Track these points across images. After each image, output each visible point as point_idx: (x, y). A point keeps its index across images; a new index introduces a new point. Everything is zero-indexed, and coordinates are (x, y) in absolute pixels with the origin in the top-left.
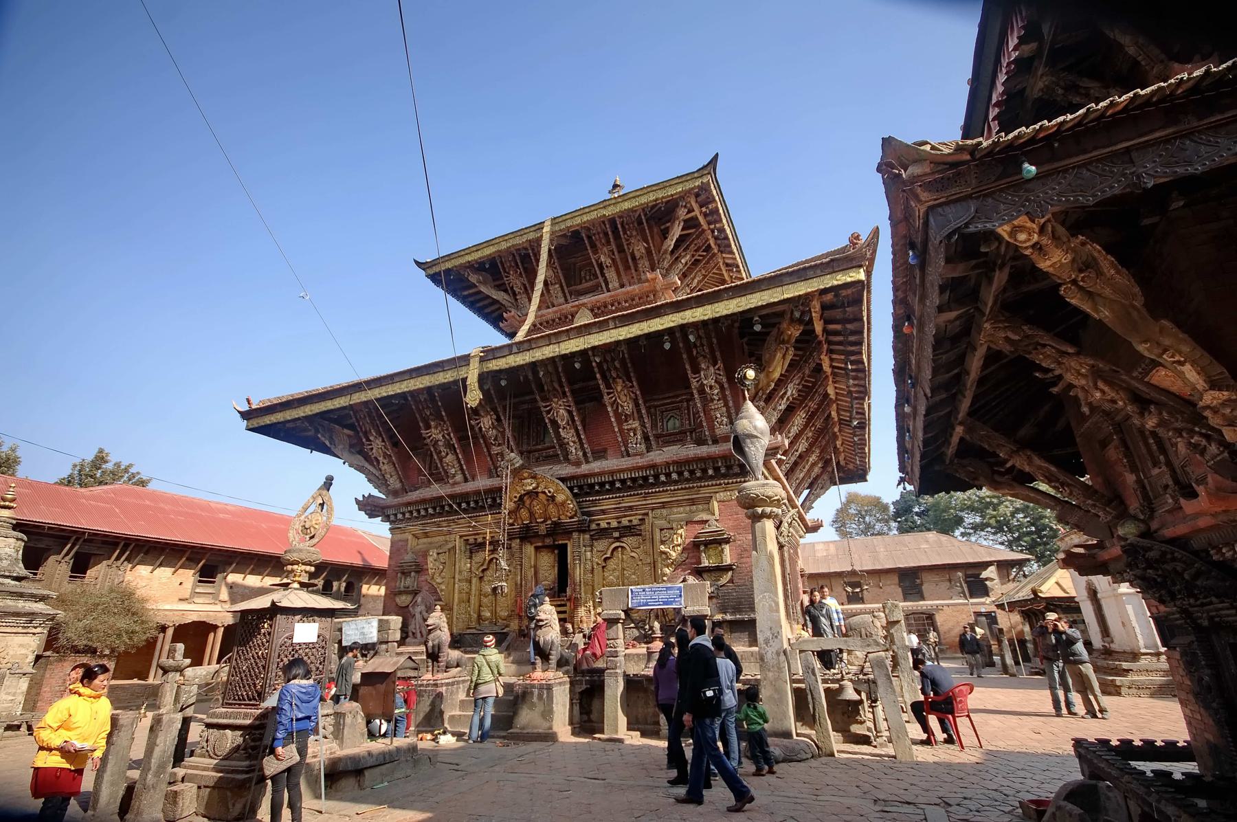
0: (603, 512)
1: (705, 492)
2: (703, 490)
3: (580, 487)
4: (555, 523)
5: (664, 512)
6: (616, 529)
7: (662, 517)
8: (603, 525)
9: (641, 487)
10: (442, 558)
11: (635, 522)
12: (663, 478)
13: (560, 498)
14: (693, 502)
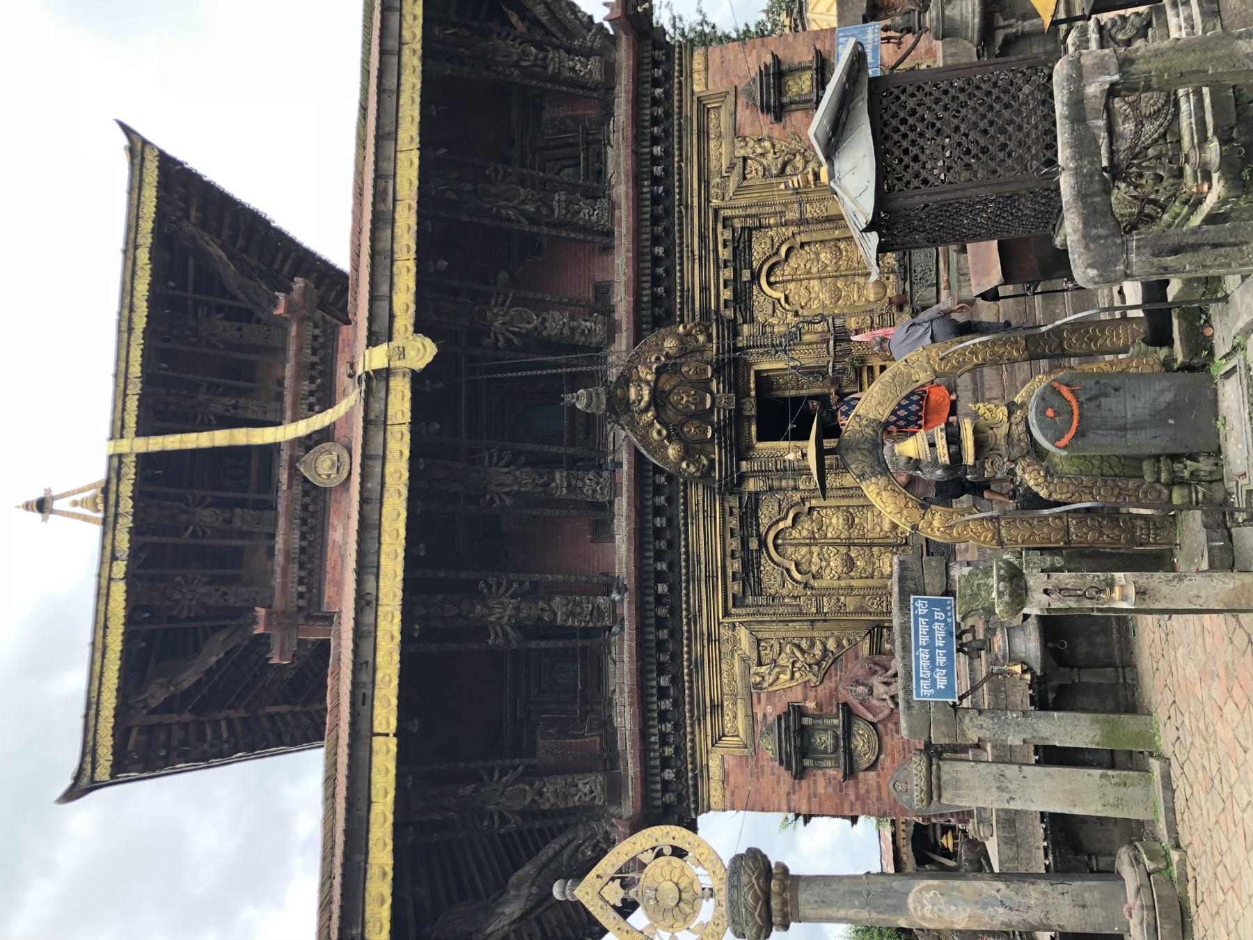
0: (704, 289)
1: (691, 110)
2: (687, 110)
5: (715, 180)
7: (723, 186)
8: (727, 294)
9: (668, 212)
10: (767, 656)
11: (728, 234)
12: (658, 170)
14: (703, 133)
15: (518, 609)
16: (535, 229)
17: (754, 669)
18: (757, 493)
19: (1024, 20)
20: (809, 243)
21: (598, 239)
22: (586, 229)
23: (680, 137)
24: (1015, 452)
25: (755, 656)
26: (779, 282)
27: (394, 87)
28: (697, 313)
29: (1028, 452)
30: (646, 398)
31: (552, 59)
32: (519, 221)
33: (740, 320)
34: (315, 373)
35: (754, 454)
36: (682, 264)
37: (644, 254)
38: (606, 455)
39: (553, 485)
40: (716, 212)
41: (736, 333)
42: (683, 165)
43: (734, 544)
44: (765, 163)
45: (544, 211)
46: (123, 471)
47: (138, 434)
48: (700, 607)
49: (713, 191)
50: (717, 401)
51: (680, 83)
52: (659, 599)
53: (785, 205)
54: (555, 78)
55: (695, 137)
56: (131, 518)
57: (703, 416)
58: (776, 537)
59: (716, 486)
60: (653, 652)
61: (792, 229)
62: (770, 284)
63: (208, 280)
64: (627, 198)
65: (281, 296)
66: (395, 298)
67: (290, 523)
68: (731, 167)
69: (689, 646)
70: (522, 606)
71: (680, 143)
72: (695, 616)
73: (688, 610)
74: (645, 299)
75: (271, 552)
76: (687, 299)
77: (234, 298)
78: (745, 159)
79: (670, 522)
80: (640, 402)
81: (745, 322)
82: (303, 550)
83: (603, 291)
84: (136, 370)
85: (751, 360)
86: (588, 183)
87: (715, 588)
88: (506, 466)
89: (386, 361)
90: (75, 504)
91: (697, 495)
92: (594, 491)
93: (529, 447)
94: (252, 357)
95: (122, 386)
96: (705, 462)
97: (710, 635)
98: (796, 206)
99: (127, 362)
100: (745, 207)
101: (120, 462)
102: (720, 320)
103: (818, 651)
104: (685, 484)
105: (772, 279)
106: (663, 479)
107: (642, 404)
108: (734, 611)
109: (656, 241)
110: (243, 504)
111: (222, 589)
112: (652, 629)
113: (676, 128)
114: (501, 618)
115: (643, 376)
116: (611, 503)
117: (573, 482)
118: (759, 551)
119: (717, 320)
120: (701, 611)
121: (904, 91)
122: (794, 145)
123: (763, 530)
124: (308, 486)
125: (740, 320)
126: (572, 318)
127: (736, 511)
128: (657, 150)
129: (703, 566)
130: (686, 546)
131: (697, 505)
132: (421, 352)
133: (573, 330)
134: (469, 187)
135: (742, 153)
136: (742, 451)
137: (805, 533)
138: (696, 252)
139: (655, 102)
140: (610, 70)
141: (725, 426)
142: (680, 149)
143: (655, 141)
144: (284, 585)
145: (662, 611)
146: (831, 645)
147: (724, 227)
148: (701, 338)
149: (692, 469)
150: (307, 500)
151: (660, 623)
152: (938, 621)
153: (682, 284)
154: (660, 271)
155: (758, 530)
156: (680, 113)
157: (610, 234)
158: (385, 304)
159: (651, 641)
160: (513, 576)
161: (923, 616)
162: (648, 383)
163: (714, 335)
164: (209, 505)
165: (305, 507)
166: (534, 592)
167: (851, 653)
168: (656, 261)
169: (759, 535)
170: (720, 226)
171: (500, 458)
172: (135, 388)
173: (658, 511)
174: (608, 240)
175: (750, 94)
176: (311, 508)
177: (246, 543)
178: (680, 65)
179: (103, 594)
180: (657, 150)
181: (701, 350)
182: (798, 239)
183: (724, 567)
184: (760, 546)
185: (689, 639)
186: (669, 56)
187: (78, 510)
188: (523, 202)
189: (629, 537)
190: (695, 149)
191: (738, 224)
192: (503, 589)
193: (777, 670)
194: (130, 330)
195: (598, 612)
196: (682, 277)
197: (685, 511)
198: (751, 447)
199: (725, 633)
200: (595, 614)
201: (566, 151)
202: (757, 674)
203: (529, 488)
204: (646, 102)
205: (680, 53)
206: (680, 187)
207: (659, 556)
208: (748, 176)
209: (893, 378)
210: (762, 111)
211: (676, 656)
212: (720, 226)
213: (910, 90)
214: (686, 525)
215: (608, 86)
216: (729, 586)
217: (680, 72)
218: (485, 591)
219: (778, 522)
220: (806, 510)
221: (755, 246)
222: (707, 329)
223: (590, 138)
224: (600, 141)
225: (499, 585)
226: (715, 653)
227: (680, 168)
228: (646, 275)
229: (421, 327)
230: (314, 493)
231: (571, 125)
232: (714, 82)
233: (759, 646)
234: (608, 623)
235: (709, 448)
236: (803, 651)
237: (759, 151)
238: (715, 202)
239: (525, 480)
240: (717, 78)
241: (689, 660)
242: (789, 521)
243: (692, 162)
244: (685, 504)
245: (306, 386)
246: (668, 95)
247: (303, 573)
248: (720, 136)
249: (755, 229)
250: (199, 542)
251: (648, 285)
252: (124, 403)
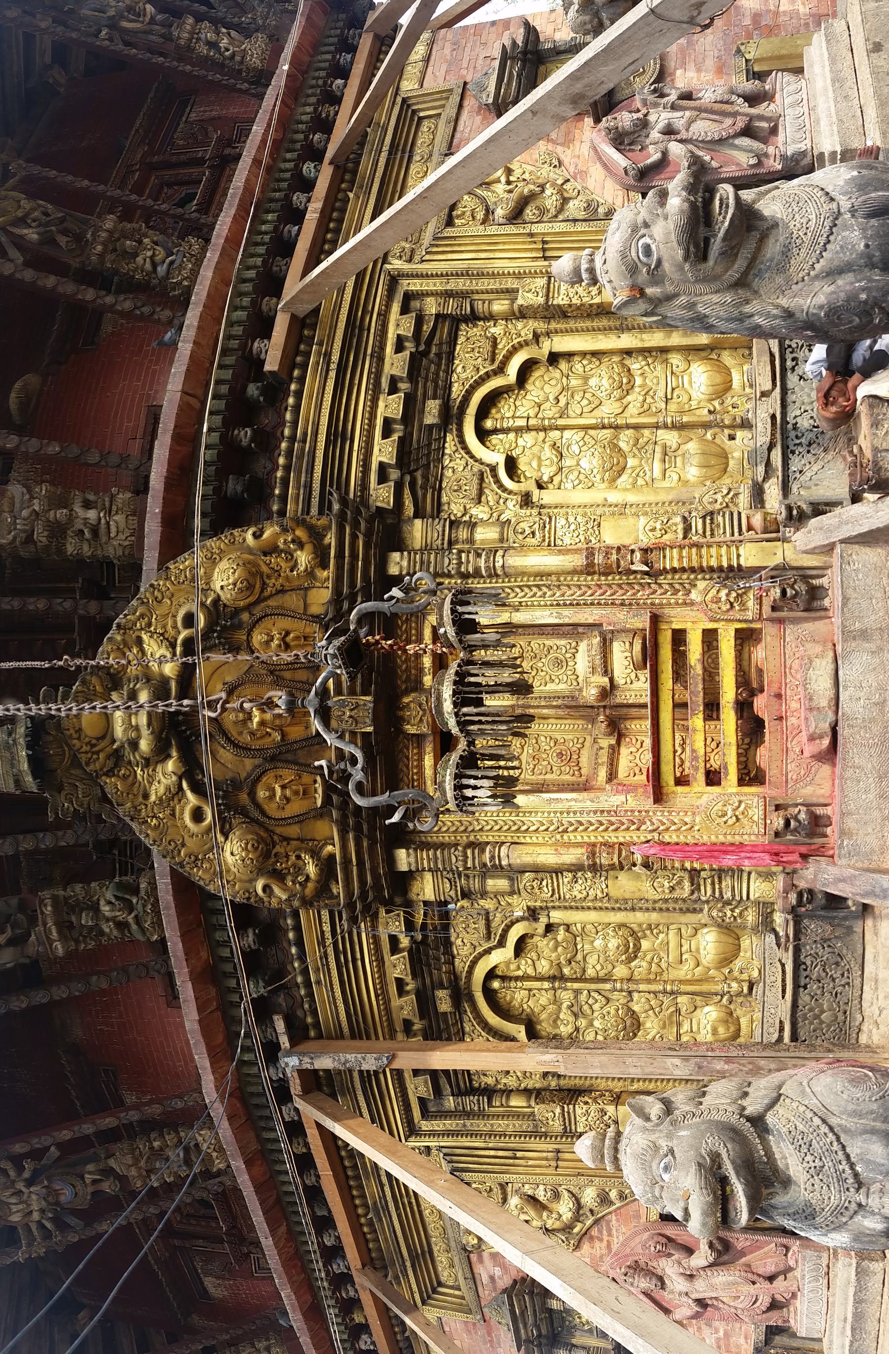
6: (412, 407)
20: (569, 356)
62: (482, 435)
105: (489, 424)
127: (405, 942)
137: (544, 967)
182: (546, 347)
219: (488, 951)
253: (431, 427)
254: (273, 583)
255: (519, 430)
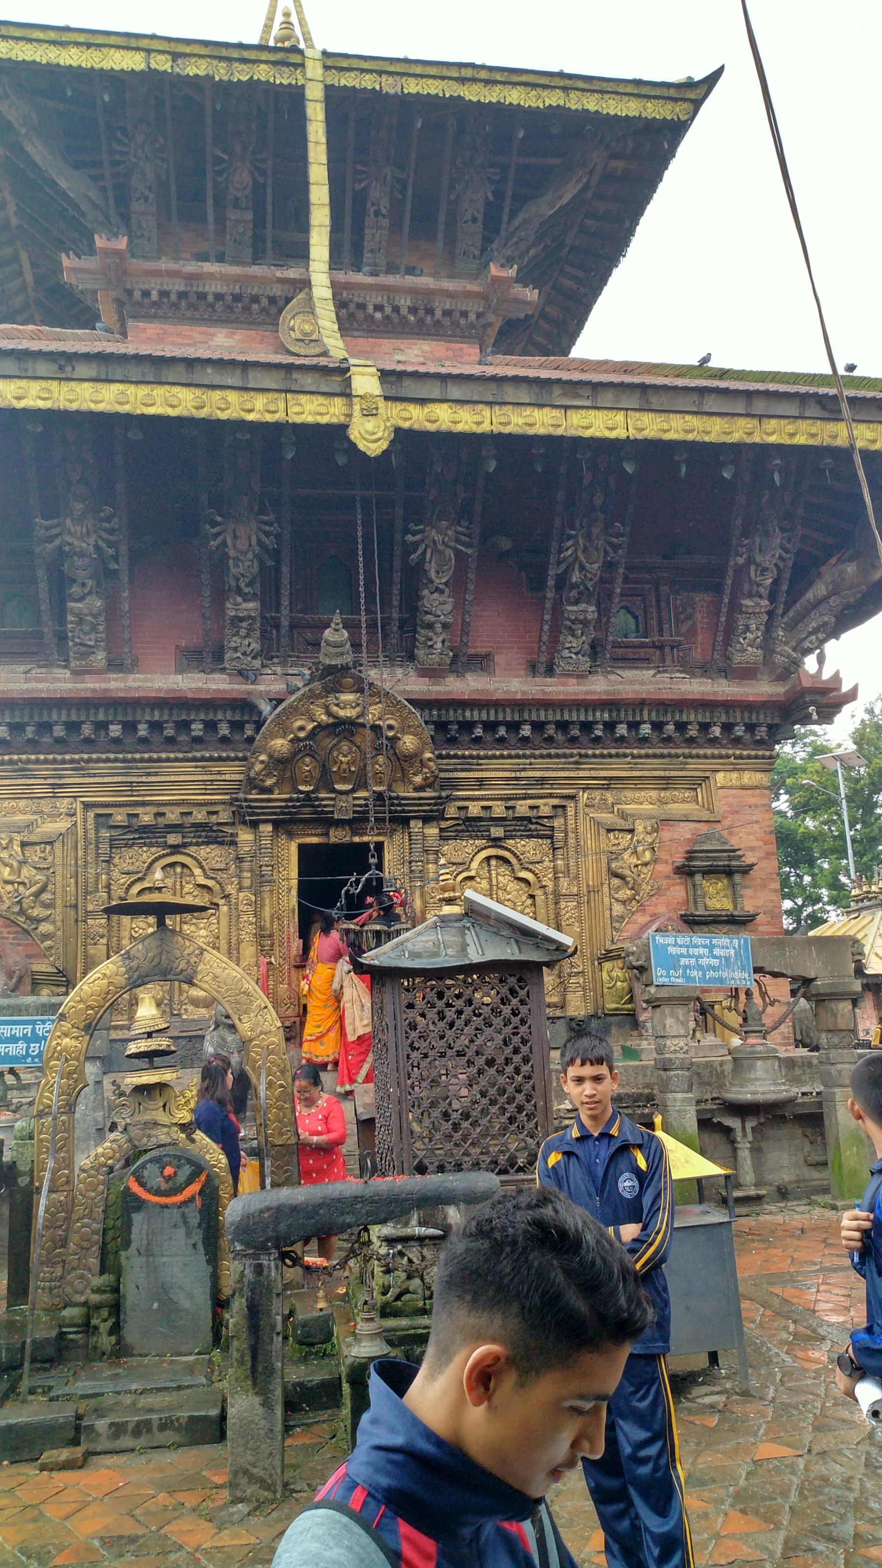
0: (481, 783)
1: (695, 768)
2: (693, 764)
3: (441, 726)
4: (379, 796)
5: (610, 797)
7: (604, 806)
8: (474, 809)
9: (573, 741)
10: (34, 855)
11: (545, 811)
12: (622, 730)
13: (409, 742)
14: (666, 783)
15: (82, 555)
16: (551, 583)
17: (18, 838)
18: (233, 843)
19: (752, 1150)
21: (543, 659)
22: (554, 643)
23: (662, 756)
24: (135, 1132)
25: (33, 838)
26: (489, 871)
27: (706, 409)
28: (451, 775)
29: (135, 1147)
30: (342, 713)
31: (758, 604)
32: (559, 563)
33: (444, 825)
34: (421, 313)
35: (283, 840)
36: (510, 757)
37: (521, 712)
38: (283, 664)
39: (239, 599)
40: (572, 797)
41: (426, 820)
42: (629, 759)
43: (173, 816)
44: (626, 856)
45: (574, 593)
46: (284, 69)
47: (330, 91)
48: (94, 775)
49: (597, 794)
50: (344, 797)
51: (728, 757)
52: (102, 726)
53: (577, 877)
54: (735, 607)
55: (662, 774)
56: (226, 78)
57: (325, 780)
58: (184, 866)
59: (241, 796)
60: (36, 719)
61: (550, 885)
62: (488, 859)
63: (533, 183)
64: (587, 693)
65: (512, 272)
66: (445, 406)
67: (236, 279)
68: (623, 816)
69: (46, 761)
70: (87, 560)
71: (655, 756)
72: (83, 769)
73: (90, 760)
74: (468, 714)
75: (203, 257)
76: (467, 763)
77: (513, 214)
78: (631, 831)
79: (197, 741)
80: (337, 705)
81: (441, 830)
82: (202, 296)
83: (482, 662)
84: (412, 87)
85: (397, 837)
86: (609, 647)
87: (119, 793)
88: (260, 543)
89: (360, 392)
90: (287, 14)
91: (232, 773)
92: (235, 649)
93: (285, 570)
94: (440, 235)
95: (392, 69)
96: (269, 782)
97: (61, 786)
98: (575, 890)
99: (422, 76)
100: (576, 830)
101: (296, 66)
102: (441, 801)
103: (36, 912)
104: (245, 759)
105: (493, 862)
106: (249, 732)
107: (335, 708)
108: (91, 815)
109: (538, 726)
110: (259, 223)
111: (151, 196)
112: (64, 718)
113: (673, 751)
114: (70, 533)
115: (372, 709)
116: (224, 670)
117: (244, 624)
118: (165, 845)
119: (440, 798)
120: (89, 776)
121: (522, 1002)
122: (646, 888)
123: (192, 850)
124: (281, 303)
125: (444, 825)
126: (445, 626)
127: (214, 819)
128: (646, 729)
129: (144, 779)
130: (168, 760)
131: (219, 773)
132: (370, 435)
133: (430, 626)
134: (598, 501)
135: (639, 827)
136: (285, 824)
138: (523, 774)
139: (704, 727)
140: (748, 673)
141: (313, 806)
142: (647, 756)
143: (658, 726)
144: (158, 273)
145: (87, 730)
146: (45, 928)
147: (555, 807)
148: (418, 779)
149: (258, 767)
150: (265, 302)
151: (73, 727)
152: (28, 1048)
153: (486, 757)
154: (502, 731)
155: (191, 844)
156: (691, 757)
157: (550, 671)
158: (436, 394)
159: (50, 715)
160: (123, 548)
161: (34, 1029)
162: (362, 715)
163: (422, 794)
164: (255, 181)
165: (255, 299)
166: (106, 574)
167: (32, 951)
168: (514, 727)
169: (185, 845)
170: (556, 802)
171: (267, 534)
172: (389, 86)
173: (210, 726)
174: (542, 669)
175: (708, 838)
176: (255, 306)
177: (211, 227)
178: (749, 757)
179: (129, 41)
180: (646, 729)
181: (405, 779)
183: (144, 804)
184: (171, 846)
185: (54, 761)
186: (760, 743)
187: (279, 18)
188: (582, 568)
189: (174, 691)
190: (647, 774)
191: (557, 823)
192: (106, 536)
193: (15, 864)
194: (462, 80)
195: (87, 652)
196: (494, 757)
197: (211, 759)
198: (291, 835)
199: (63, 805)
200: (83, 649)
201: (654, 622)
202: (11, 841)
203: (234, 571)
204: (704, 717)
205: (763, 757)
206: (602, 756)
207: (156, 726)
208: (611, 835)
209: (246, 993)
210: (688, 852)
211: (33, 745)
212: (556, 802)
213: (523, 1010)
214: (195, 759)
215: (727, 672)
216: (121, 810)
217: (741, 757)
218: (102, 514)
219: (202, 867)
220: (215, 900)
221: (533, 842)
222: (430, 786)
223: (667, 650)
224: (663, 661)
225: (111, 532)
226: (39, 791)
227: (625, 756)
228: (496, 713)
229: (405, 439)
230: (273, 310)
231: (684, 629)
232: (726, 797)
233: (46, 843)
234: (73, 664)
235: (287, 787)
236: (37, 894)
237: (640, 849)
238: (584, 797)
239: (244, 567)
240: (731, 800)
241: (29, 761)
242: (202, 880)
243: (631, 769)
244: (220, 759)
245: (405, 302)
246: (714, 742)
247: (173, 297)
248: (662, 802)
249: (552, 843)
250: (209, 167)
251: (484, 717)
252: (370, 71)
253: (489, 831)
254: (406, 765)
255: (490, 879)
